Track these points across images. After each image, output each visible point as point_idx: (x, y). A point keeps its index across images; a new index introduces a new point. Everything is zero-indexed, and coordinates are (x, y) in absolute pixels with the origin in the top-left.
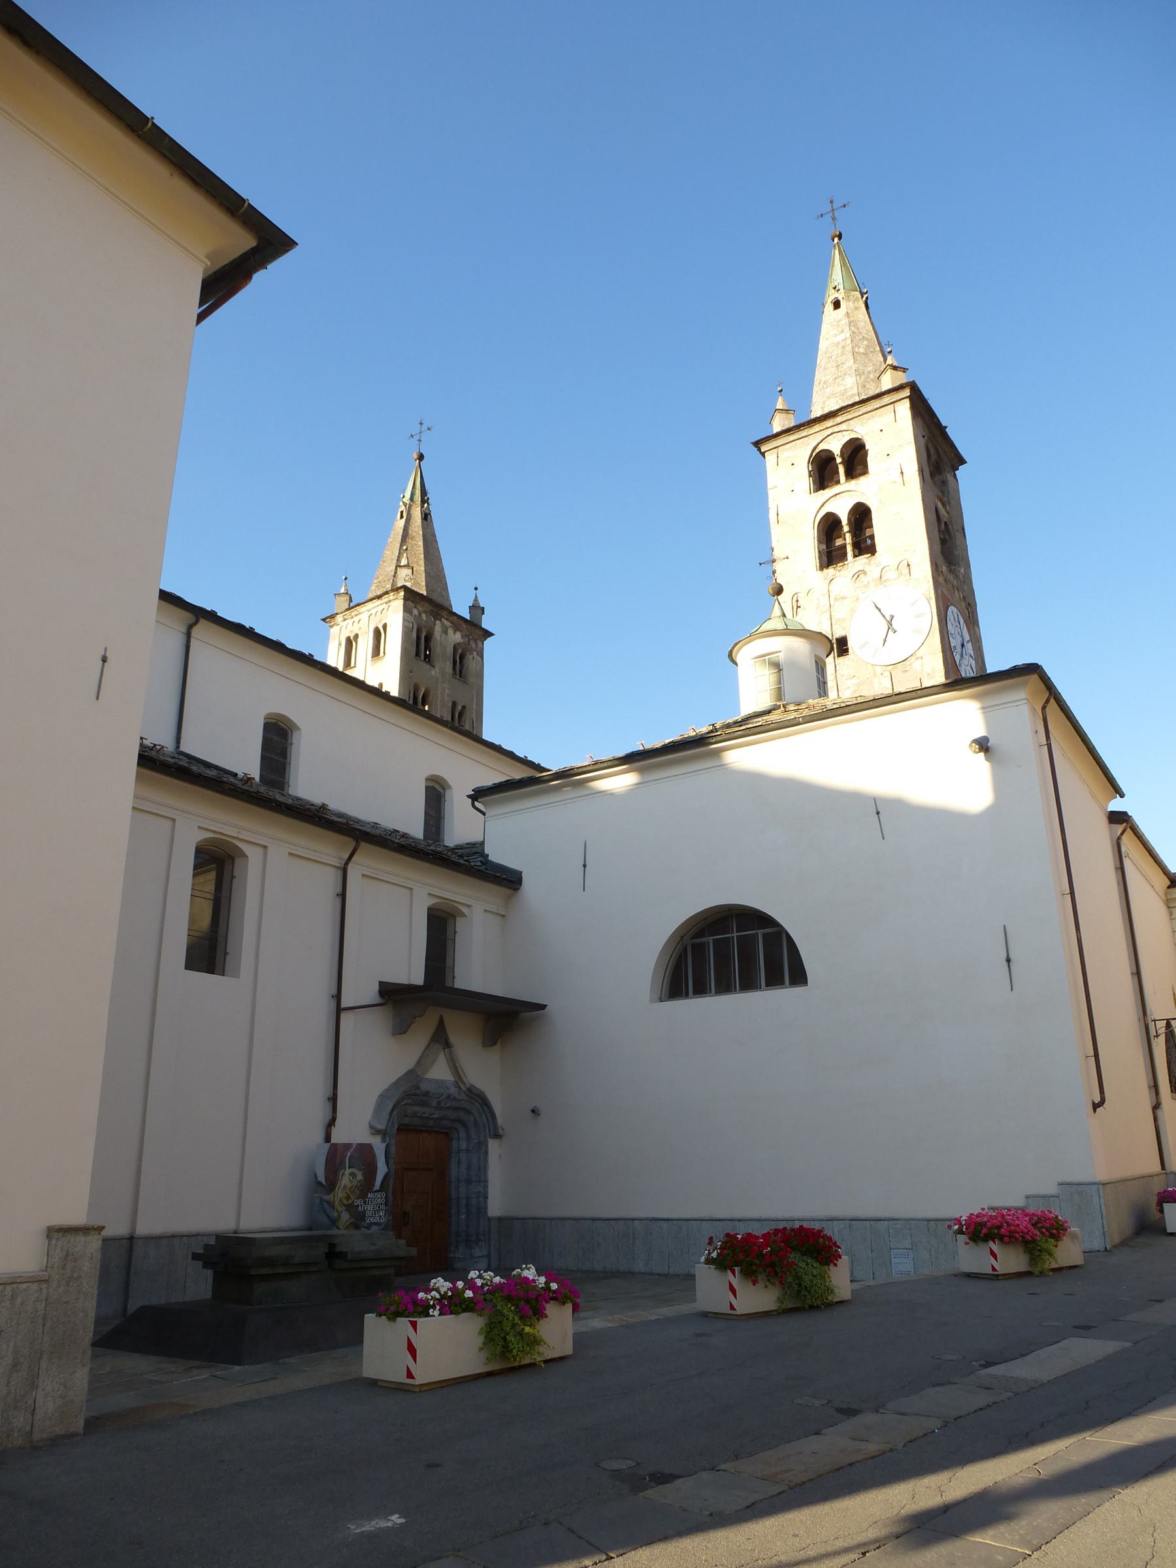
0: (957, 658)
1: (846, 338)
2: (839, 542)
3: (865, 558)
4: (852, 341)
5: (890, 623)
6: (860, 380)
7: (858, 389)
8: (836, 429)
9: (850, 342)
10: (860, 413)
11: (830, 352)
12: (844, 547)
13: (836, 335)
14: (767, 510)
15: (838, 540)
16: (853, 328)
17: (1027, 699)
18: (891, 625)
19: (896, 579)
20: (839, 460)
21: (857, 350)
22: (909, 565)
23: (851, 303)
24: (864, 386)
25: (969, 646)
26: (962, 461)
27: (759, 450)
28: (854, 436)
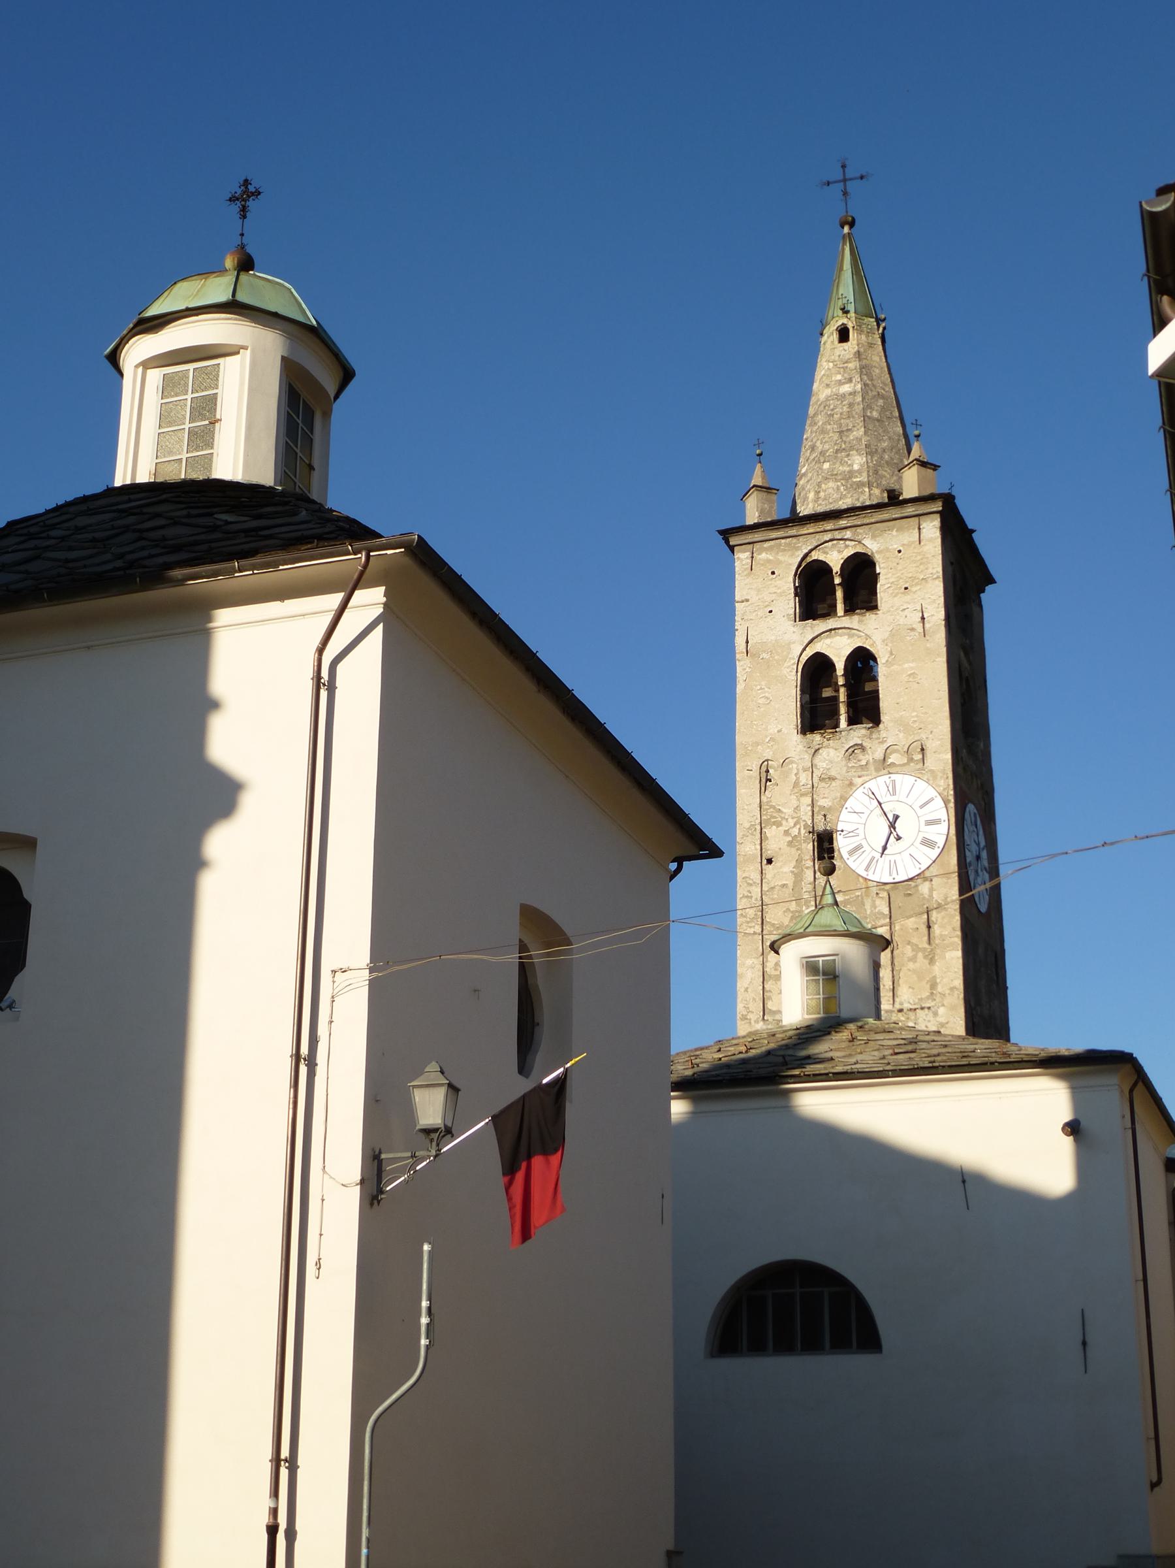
0: (972, 878)
1: (855, 392)
2: (827, 693)
3: (865, 728)
4: (863, 399)
5: (892, 826)
6: (872, 461)
7: (869, 476)
8: (837, 535)
9: (861, 399)
10: (873, 520)
11: (832, 407)
12: (835, 700)
13: (840, 383)
14: (732, 632)
15: (827, 689)
16: (865, 378)
17: (1118, 1085)
18: (895, 829)
19: (904, 765)
20: (837, 580)
21: (869, 414)
22: (922, 750)
23: (863, 337)
24: (876, 472)
25: (984, 854)
26: (991, 580)
27: (727, 542)
28: (860, 549)
